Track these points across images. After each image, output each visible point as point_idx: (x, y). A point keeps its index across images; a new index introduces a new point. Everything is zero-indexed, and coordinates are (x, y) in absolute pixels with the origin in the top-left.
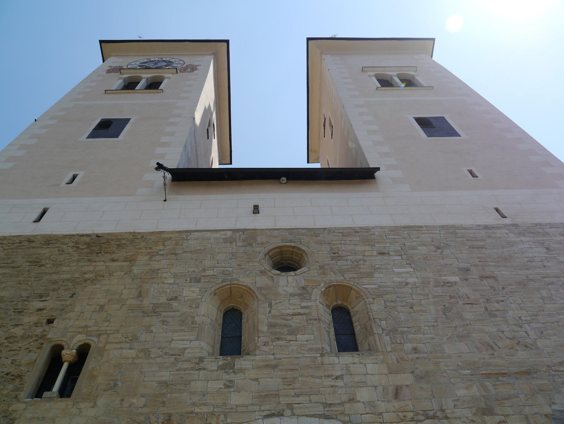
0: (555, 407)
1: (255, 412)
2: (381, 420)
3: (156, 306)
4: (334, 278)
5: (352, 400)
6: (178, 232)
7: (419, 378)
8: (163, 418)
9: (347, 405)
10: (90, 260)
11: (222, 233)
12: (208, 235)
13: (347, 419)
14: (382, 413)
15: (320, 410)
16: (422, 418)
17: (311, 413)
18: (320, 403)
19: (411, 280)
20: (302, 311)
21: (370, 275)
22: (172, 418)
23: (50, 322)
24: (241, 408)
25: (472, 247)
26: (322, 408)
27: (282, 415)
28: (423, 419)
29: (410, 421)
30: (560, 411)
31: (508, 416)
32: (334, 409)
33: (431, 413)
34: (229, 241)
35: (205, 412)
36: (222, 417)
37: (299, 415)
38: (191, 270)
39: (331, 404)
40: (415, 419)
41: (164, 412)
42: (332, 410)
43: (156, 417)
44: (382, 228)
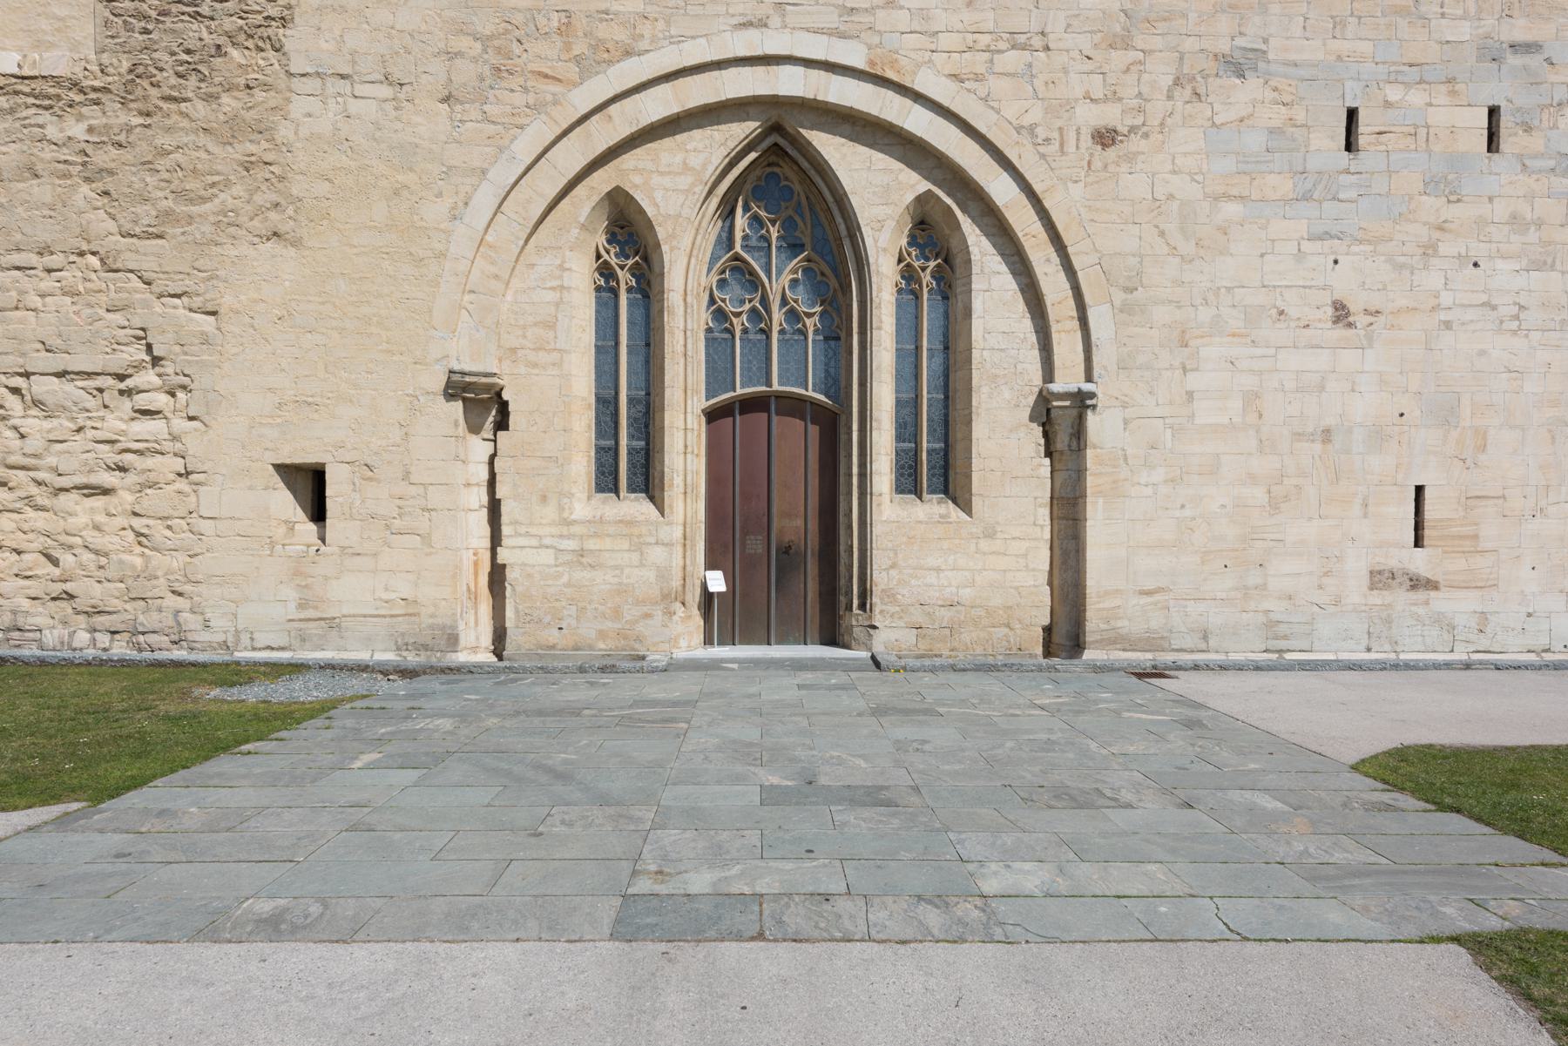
0: (1240, 42)
1: (719, 15)
2: (933, 47)
8: (556, 19)
9: (881, 14)
13: (876, 40)
14: (937, 33)
15: (831, 19)
16: (1002, 45)
17: (816, 26)
18: (833, 5)
22: (573, 20)
24: (694, 7)
26: (835, 17)
27: (766, 25)
28: (1004, 48)
29: (983, 51)
30: (1245, 49)
31: (1152, 52)
32: (855, 18)
33: (1022, 39)
35: (629, 12)
36: (661, 25)
37: (794, 29)
39: (852, 9)
40: (993, 48)
41: (557, 8)
42: (853, 22)
43: (544, 16)
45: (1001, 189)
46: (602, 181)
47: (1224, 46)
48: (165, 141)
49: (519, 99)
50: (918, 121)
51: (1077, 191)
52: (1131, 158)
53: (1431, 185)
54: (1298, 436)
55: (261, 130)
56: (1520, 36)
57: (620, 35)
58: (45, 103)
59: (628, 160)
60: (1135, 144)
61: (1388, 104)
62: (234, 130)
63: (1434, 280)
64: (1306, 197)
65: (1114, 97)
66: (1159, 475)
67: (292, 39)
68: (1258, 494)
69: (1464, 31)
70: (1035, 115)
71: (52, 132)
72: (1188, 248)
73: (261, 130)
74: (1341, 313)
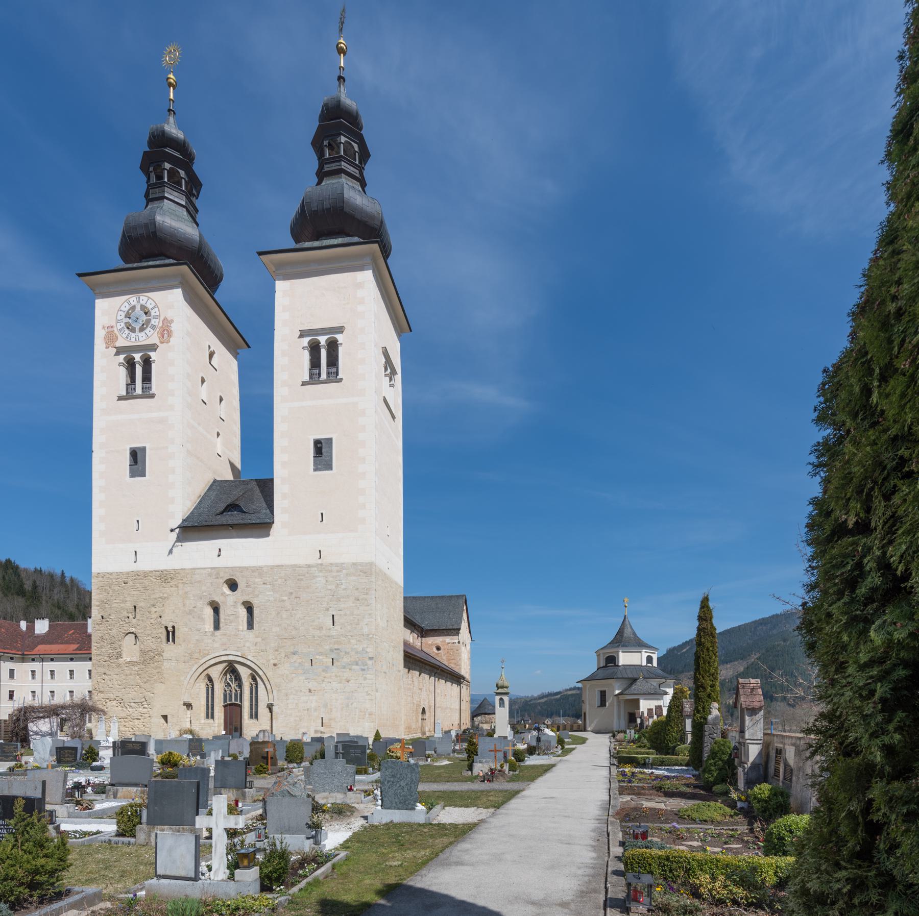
3: (190, 610)
4: (246, 598)
5: (244, 646)
6: (191, 569)
7: (263, 639)
10: (163, 587)
11: (207, 570)
12: (202, 571)
19: (271, 599)
20: (234, 613)
21: (257, 596)
23: (161, 617)
25: (298, 580)
34: (210, 575)
38: (199, 592)
44: (268, 566)
45: (260, 673)
46: (205, 673)
47: (292, 650)
48: (147, 670)
49: (193, 662)
50: (248, 663)
51: (271, 673)
52: (278, 668)
53: (324, 671)
54: (304, 710)
55: (160, 668)
56: (336, 648)
57: (207, 652)
58: (133, 665)
59: (209, 670)
60: (279, 666)
61: (316, 659)
62: (156, 668)
63: (323, 685)
64: (304, 673)
65: (276, 659)
66: (283, 716)
67: (164, 654)
68: (298, 719)
69: (327, 647)
70: (265, 662)
71: (134, 669)
72: (287, 681)
73: (160, 668)
74: (310, 691)
